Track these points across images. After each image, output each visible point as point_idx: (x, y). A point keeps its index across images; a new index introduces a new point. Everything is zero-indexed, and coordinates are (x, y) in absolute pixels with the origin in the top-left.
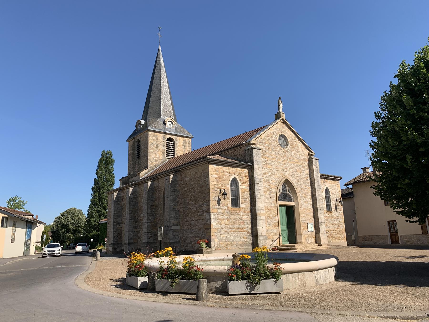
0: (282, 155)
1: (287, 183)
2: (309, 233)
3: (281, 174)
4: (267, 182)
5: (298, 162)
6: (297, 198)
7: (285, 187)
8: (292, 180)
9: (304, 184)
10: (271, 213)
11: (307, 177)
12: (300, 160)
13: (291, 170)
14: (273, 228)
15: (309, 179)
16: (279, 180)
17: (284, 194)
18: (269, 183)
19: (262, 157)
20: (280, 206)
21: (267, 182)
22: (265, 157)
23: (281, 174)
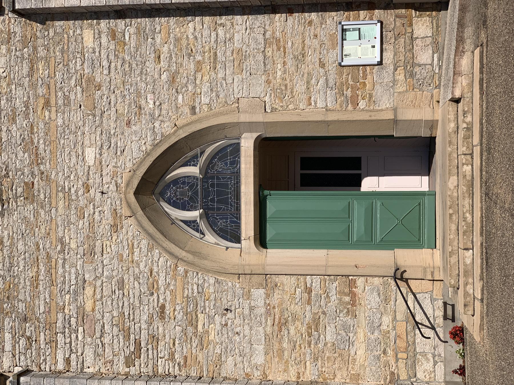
0: (29, 210)
1: (153, 186)
2: (388, 56)
3: (115, 228)
4: (159, 327)
5: (47, 104)
6: (222, 127)
7: (176, 181)
8: (137, 150)
9: (150, 65)
10: (295, 318)
11: (113, 34)
12: (33, 86)
13: (90, 154)
14: (361, 316)
15: (121, 23)
16: (144, 242)
17: (206, 194)
18: (163, 307)
19: (52, 342)
20: (262, 240)
21: (159, 327)
22: (50, 326)
23: (115, 228)
